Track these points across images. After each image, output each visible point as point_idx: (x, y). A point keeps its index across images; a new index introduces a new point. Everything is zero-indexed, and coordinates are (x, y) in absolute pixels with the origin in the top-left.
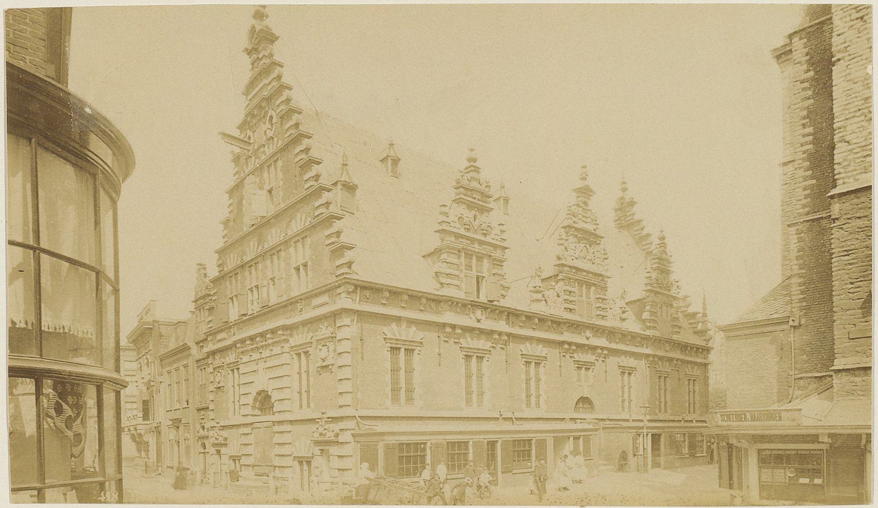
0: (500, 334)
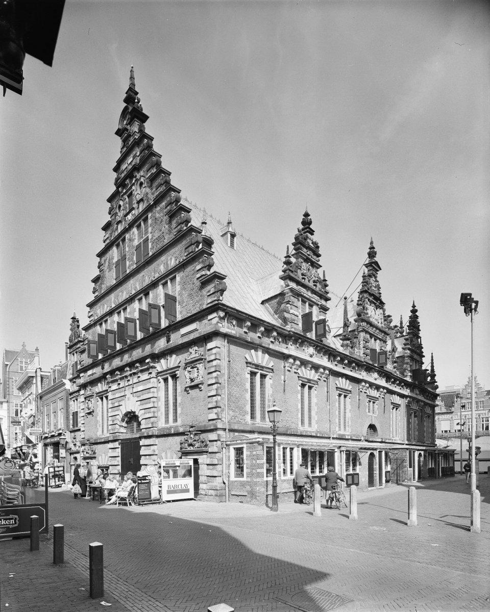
0: (325, 368)
